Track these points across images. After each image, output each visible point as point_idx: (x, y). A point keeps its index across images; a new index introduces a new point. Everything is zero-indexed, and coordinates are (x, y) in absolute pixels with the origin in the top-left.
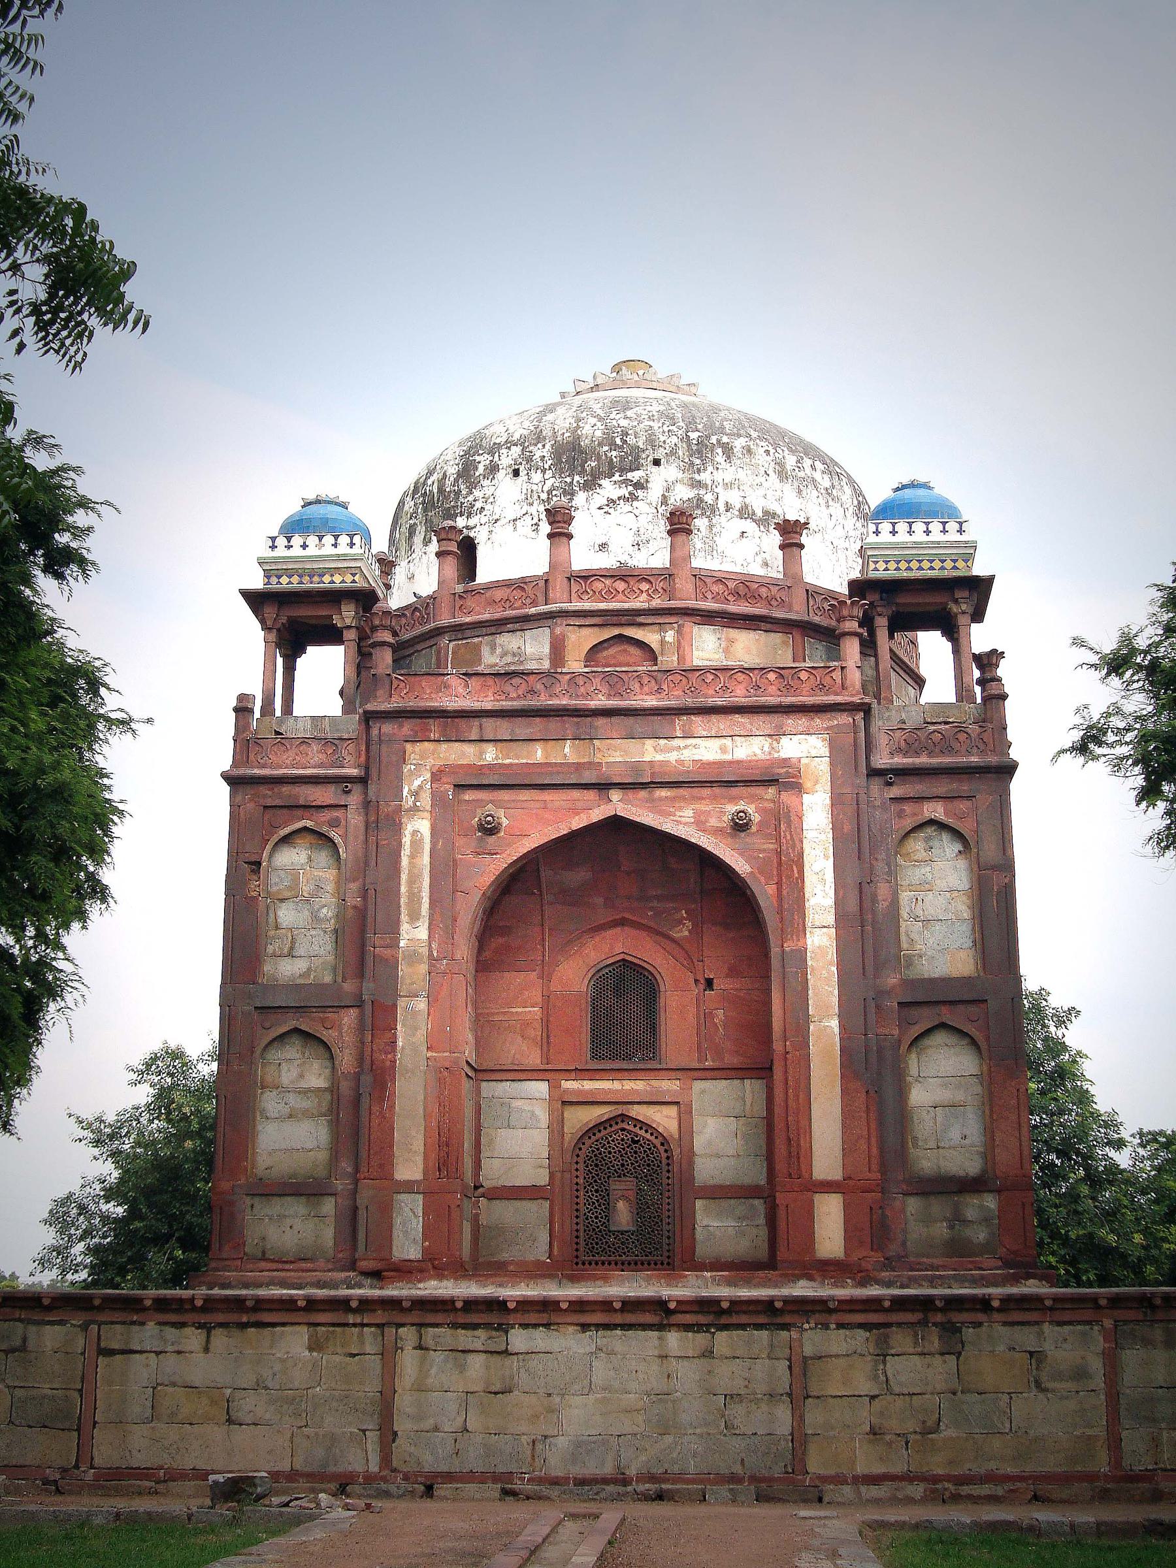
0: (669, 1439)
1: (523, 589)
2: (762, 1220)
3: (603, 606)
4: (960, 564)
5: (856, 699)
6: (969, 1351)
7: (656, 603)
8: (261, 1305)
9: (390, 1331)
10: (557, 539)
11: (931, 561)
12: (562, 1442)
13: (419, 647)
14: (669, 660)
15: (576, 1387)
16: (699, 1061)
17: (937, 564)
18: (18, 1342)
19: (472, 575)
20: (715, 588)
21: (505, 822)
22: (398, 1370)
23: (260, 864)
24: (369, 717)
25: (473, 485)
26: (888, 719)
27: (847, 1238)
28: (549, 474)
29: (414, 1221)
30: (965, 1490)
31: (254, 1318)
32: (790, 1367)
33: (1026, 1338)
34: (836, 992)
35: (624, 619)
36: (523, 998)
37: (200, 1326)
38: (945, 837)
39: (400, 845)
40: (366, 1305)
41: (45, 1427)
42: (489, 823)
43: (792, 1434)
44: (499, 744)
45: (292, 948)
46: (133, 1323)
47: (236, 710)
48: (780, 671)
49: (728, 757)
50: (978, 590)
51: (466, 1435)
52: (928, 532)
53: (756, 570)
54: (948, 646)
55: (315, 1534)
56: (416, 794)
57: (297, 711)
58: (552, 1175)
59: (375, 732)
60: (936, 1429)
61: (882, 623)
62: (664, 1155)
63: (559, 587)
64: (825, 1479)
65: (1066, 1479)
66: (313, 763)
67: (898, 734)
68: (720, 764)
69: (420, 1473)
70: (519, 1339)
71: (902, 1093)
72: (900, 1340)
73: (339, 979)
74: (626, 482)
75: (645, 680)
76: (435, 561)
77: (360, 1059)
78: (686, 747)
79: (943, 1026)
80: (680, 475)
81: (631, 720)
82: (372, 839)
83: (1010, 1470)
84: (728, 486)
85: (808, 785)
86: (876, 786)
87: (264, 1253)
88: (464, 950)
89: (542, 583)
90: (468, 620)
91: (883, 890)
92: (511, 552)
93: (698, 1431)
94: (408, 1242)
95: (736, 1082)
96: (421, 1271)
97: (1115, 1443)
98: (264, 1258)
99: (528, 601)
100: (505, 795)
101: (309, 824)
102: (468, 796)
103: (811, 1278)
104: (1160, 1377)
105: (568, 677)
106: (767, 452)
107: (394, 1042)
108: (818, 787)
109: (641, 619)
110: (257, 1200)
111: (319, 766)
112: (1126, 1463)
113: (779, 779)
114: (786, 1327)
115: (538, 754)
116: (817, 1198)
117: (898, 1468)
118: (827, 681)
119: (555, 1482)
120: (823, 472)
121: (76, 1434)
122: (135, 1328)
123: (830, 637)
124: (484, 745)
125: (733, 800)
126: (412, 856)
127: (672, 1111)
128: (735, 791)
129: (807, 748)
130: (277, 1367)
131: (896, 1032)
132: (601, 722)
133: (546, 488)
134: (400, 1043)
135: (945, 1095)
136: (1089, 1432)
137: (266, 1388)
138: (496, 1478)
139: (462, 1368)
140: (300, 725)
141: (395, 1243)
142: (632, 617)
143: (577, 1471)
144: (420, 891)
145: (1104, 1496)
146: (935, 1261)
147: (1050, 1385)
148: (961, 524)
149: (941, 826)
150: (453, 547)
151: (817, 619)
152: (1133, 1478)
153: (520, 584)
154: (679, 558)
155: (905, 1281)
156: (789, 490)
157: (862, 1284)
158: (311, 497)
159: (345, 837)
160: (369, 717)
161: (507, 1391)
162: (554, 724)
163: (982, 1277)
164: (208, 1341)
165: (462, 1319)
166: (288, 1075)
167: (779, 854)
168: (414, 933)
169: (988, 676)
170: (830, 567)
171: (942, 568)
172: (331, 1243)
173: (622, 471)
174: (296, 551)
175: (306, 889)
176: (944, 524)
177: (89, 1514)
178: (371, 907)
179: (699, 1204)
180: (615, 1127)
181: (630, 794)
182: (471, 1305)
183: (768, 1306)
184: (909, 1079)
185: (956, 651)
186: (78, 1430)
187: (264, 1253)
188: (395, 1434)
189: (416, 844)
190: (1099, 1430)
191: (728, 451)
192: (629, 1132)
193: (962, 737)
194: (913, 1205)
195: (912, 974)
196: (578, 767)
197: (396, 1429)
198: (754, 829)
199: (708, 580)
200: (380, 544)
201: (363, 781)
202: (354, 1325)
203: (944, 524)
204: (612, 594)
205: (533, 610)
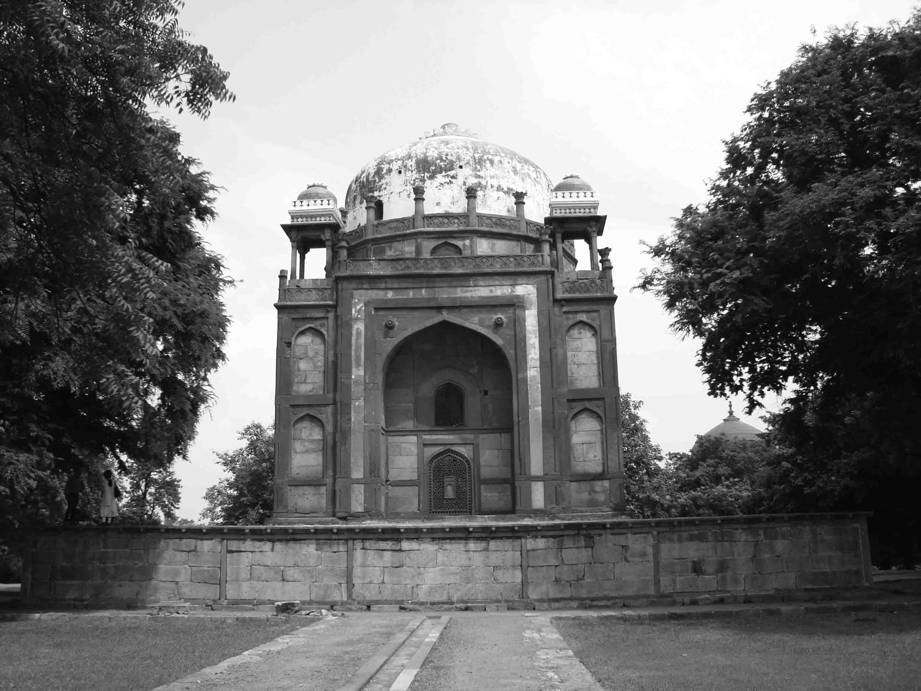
0: (470, 585)
3: (438, 229)
5: (548, 269)
6: (596, 546)
7: (461, 228)
8: (295, 531)
9: (350, 543)
12: (425, 587)
14: (467, 253)
15: (431, 564)
18: (193, 548)
21: (397, 324)
23: (290, 343)
24: (338, 280)
25: (381, 178)
30: (595, 603)
33: (621, 540)
36: (406, 399)
37: (270, 541)
38: (587, 328)
40: (340, 531)
47: (280, 277)
48: (515, 257)
50: (599, 222)
53: (504, 213)
54: (588, 245)
55: (320, 627)
56: (359, 311)
57: (306, 277)
59: (340, 286)
60: (583, 578)
61: (559, 236)
63: (419, 222)
66: (313, 299)
70: (405, 545)
71: (568, 438)
72: (568, 542)
79: (586, 410)
80: (471, 172)
83: (613, 595)
84: (492, 177)
85: (528, 306)
88: (380, 379)
91: (560, 351)
92: (398, 207)
94: (357, 506)
95: (498, 435)
97: (657, 582)
100: (395, 313)
101: (312, 325)
103: (530, 517)
104: (676, 554)
110: (292, 488)
112: (662, 589)
113: (515, 305)
114: (519, 538)
117: (568, 595)
118: (535, 261)
119: (422, 604)
126: (357, 340)
127: (471, 448)
129: (526, 290)
130: (303, 558)
131: (566, 412)
132: (437, 279)
134: (353, 419)
135: (587, 439)
138: (397, 602)
139: (382, 557)
142: (451, 234)
143: (431, 599)
145: (653, 604)
146: (584, 509)
150: (373, 205)
151: (530, 235)
152: (666, 596)
153: (402, 221)
154: (471, 208)
156: (518, 178)
158: (311, 184)
159: (327, 331)
166: (305, 434)
167: (515, 336)
168: (358, 373)
170: (537, 212)
172: (325, 505)
173: (446, 171)
174: (305, 208)
175: (311, 354)
177: (225, 618)
179: (482, 486)
182: (385, 530)
183: (512, 529)
185: (591, 248)
189: (358, 333)
190: (650, 577)
191: (492, 162)
195: (574, 388)
196: (428, 300)
200: (341, 204)
201: (335, 307)
204: (442, 224)
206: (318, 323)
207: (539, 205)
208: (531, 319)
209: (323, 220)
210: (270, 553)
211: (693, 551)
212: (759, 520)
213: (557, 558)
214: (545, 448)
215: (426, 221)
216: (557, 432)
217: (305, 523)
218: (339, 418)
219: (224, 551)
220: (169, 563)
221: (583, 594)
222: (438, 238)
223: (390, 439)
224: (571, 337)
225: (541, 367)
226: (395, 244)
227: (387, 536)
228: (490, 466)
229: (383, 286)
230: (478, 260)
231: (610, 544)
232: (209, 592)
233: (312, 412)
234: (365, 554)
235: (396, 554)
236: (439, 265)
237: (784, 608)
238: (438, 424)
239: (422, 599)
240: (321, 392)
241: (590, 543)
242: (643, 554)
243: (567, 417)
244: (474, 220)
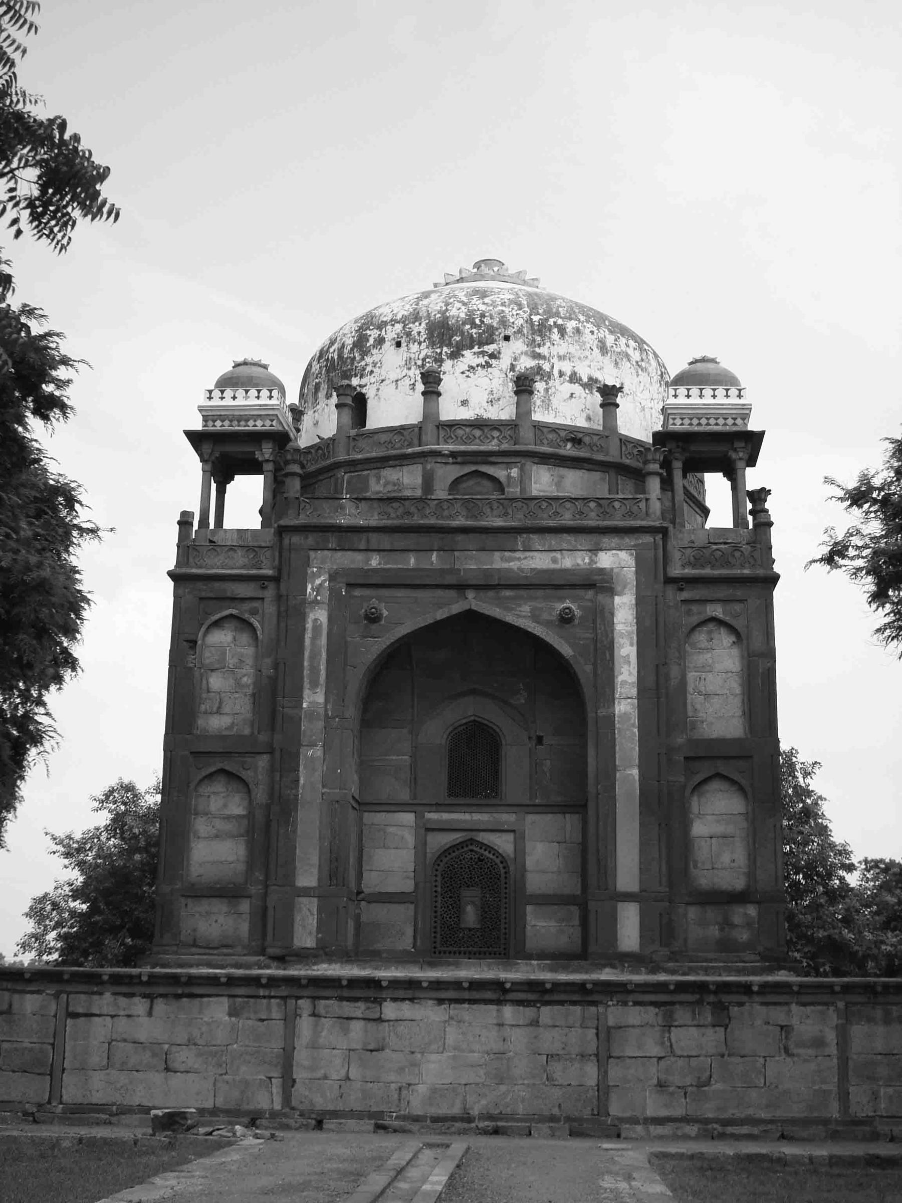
0: (503, 1088)
1: (402, 434)
2: (576, 922)
3: (463, 448)
4: (739, 421)
5: (657, 524)
7: (505, 446)
8: (192, 980)
10: (429, 397)
11: (717, 419)
12: (422, 1089)
13: (321, 478)
14: (514, 491)
15: (434, 1047)
16: (531, 799)
17: (721, 421)
18: (5, 1007)
19: (363, 423)
20: (550, 436)
21: (385, 613)
22: (297, 1030)
23: (195, 642)
25: (365, 353)
26: (682, 539)
27: (641, 937)
28: (424, 345)
29: (311, 918)
30: (730, 1130)
31: (187, 990)
32: (597, 1034)
33: (778, 1015)
34: (637, 748)
35: (479, 459)
36: (397, 750)
37: (145, 996)
38: (723, 630)
39: (304, 629)
40: (273, 982)
41: (25, 1071)
42: (373, 614)
43: (598, 1085)
44: (382, 553)
45: (219, 708)
46: (94, 993)
47: (179, 523)
49: (558, 566)
50: (752, 442)
51: (348, 1083)
52: (714, 396)
53: (582, 423)
55: (232, 1156)
56: (318, 589)
57: (227, 525)
58: (416, 885)
59: (286, 541)
60: (708, 1083)
61: (677, 465)
62: (503, 871)
63: (430, 433)
64: (622, 1120)
65: (806, 1122)
66: (238, 564)
67: (689, 551)
69: (312, 1111)
70: (390, 1010)
72: (682, 1015)
73: (256, 732)
74: (483, 353)
75: (495, 505)
76: (335, 411)
77: (271, 795)
78: (525, 558)
80: (525, 348)
81: (484, 536)
82: (283, 625)
83: (763, 1115)
84: (561, 358)
85: (619, 588)
86: (670, 591)
87: (195, 940)
88: (352, 712)
89: (416, 430)
90: (359, 456)
91: (674, 671)
92: (393, 405)
93: (526, 1082)
94: (305, 935)
95: (560, 816)
96: (315, 956)
97: (844, 1096)
98: (195, 945)
99: (406, 443)
101: (234, 612)
102: (357, 592)
103: (613, 967)
104: (879, 1045)
105: (435, 502)
106: (592, 332)
108: (626, 591)
109: (493, 459)
110: (189, 900)
111: (244, 567)
114: (594, 1003)
115: (412, 562)
116: (620, 905)
117: (679, 1112)
119: (416, 1119)
120: (635, 349)
121: (49, 1077)
122: (96, 997)
123: (638, 476)
124: (370, 553)
125: (562, 599)
126: (314, 638)
127: (510, 837)
128: (561, 593)
129: (617, 559)
130: (204, 1029)
132: (460, 538)
133: (421, 356)
134: (302, 781)
135: (720, 829)
136: (824, 1087)
137: (195, 1044)
138: (371, 1115)
139: (346, 1031)
140: (228, 535)
141: (295, 935)
142: (486, 457)
143: (433, 1111)
144: (319, 665)
145: (834, 1137)
146: (711, 955)
147: (795, 1051)
148: (740, 390)
149: (720, 622)
150: (349, 401)
153: (400, 430)
154: (523, 410)
155: (686, 970)
156: (607, 361)
157: (653, 971)
158: (240, 359)
159: (262, 623)
160: (282, 531)
161: (383, 1050)
162: (424, 540)
163: (744, 968)
164: (151, 1008)
165: (346, 993)
166: (215, 805)
167: (595, 641)
168: (314, 698)
169: (758, 508)
170: (639, 420)
171: (725, 424)
173: (481, 344)
175: (231, 661)
176: (727, 390)
177: (59, 1139)
179: (529, 908)
180: (466, 849)
181: (482, 594)
182: (354, 983)
183: (581, 987)
184: (692, 816)
185: (734, 488)
186: (51, 1075)
187: (195, 940)
188: (294, 1081)
189: (317, 628)
190: (832, 1086)
191: (562, 330)
192: (476, 852)
194: (693, 913)
196: (442, 571)
197: (295, 1077)
198: (576, 621)
199: (545, 430)
200: (293, 397)
201: (276, 579)
202: (264, 997)
203: (727, 390)
204: (470, 439)
205: (410, 450)
206: (247, 606)
207: (643, 409)
208: (624, 611)
209: (259, 426)
210: (144, 1020)
213: (663, 1043)
214: (644, 845)
216: (666, 813)
217: (210, 965)
219: (62, 1014)
223: (370, 818)
224: (693, 646)
227: (357, 993)
228: (544, 872)
229: (362, 547)
231: (758, 1022)
232: (30, 1089)
234: (316, 1025)
235: (370, 1025)
238: (452, 793)
241: (722, 1018)
243: (684, 787)
244: (526, 434)
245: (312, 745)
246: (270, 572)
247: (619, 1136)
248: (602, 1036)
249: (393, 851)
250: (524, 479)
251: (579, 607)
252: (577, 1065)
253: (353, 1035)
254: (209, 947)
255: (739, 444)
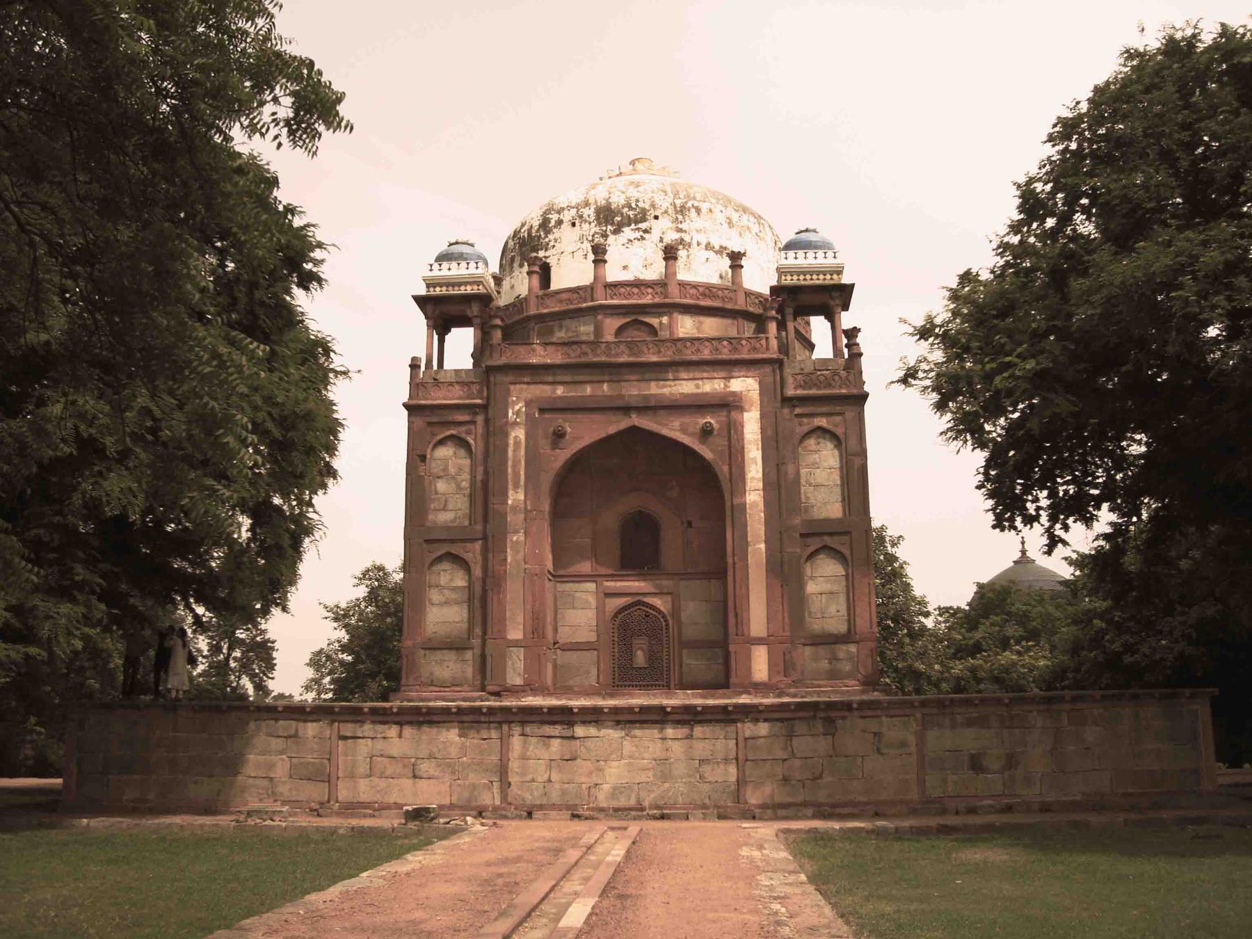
0: (667, 785)
2: (720, 661)
3: (624, 302)
5: (775, 356)
7: (657, 300)
8: (431, 711)
9: (505, 727)
14: (665, 334)
18: (292, 732)
21: (569, 430)
24: (490, 370)
25: (548, 231)
30: (838, 810)
31: (428, 718)
33: (873, 725)
38: (827, 436)
39: (507, 445)
40: (491, 710)
48: (730, 340)
49: (700, 391)
53: (715, 280)
54: (829, 324)
55: (465, 839)
56: (518, 413)
57: (446, 366)
59: (492, 379)
60: (820, 777)
61: (789, 311)
63: (600, 291)
66: (453, 397)
68: (697, 395)
69: (524, 805)
70: (580, 731)
71: (801, 586)
72: (800, 727)
74: (638, 229)
77: (485, 569)
79: (825, 548)
80: (670, 225)
82: (491, 440)
88: (546, 506)
90: (546, 311)
91: (791, 469)
92: (572, 270)
100: (569, 416)
101: (454, 432)
107: (505, 560)
111: (460, 398)
113: (729, 405)
114: (734, 721)
116: (753, 647)
117: (800, 799)
118: (758, 345)
119: (602, 810)
123: (760, 321)
125: (703, 417)
126: (514, 451)
127: (669, 598)
129: (745, 385)
131: (798, 550)
135: (827, 587)
138: (568, 808)
139: (548, 746)
141: (508, 677)
143: (615, 804)
145: (914, 812)
146: (822, 683)
147: (884, 751)
150: (537, 269)
151: (751, 309)
154: (669, 273)
157: (779, 696)
159: (475, 440)
166: (444, 579)
167: (730, 447)
168: (516, 497)
170: (759, 278)
173: (636, 223)
174: (445, 272)
175: (452, 471)
177: (337, 828)
178: (491, 481)
179: (685, 652)
182: (552, 710)
185: (833, 328)
189: (517, 443)
191: (698, 210)
193: (837, 378)
194: (808, 650)
196: (611, 397)
200: (494, 267)
201: (485, 408)
204: (630, 295)
206: (463, 428)
207: (762, 269)
208: (751, 424)
209: (469, 290)
211: (969, 740)
212: (1061, 699)
213: (785, 748)
215: (609, 291)
216: (786, 575)
217: (444, 699)
218: (490, 556)
220: (262, 753)
221: (822, 797)
222: (625, 315)
223: (561, 587)
225: (764, 489)
226: (567, 322)
228: (696, 623)
229: (550, 379)
230: (679, 344)
233: (455, 549)
234: (525, 742)
235: (566, 742)
236: (627, 351)
237: (1093, 818)
239: (604, 805)
240: (467, 523)
242: (903, 744)
243: (800, 557)
244: (674, 290)
245: (516, 532)
246: (479, 401)
247: (754, 818)
248: (741, 745)
249: (580, 612)
250: (670, 325)
251: (717, 422)
252: (722, 766)
253: (553, 749)
254: (443, 685)
255: (835, 294)
